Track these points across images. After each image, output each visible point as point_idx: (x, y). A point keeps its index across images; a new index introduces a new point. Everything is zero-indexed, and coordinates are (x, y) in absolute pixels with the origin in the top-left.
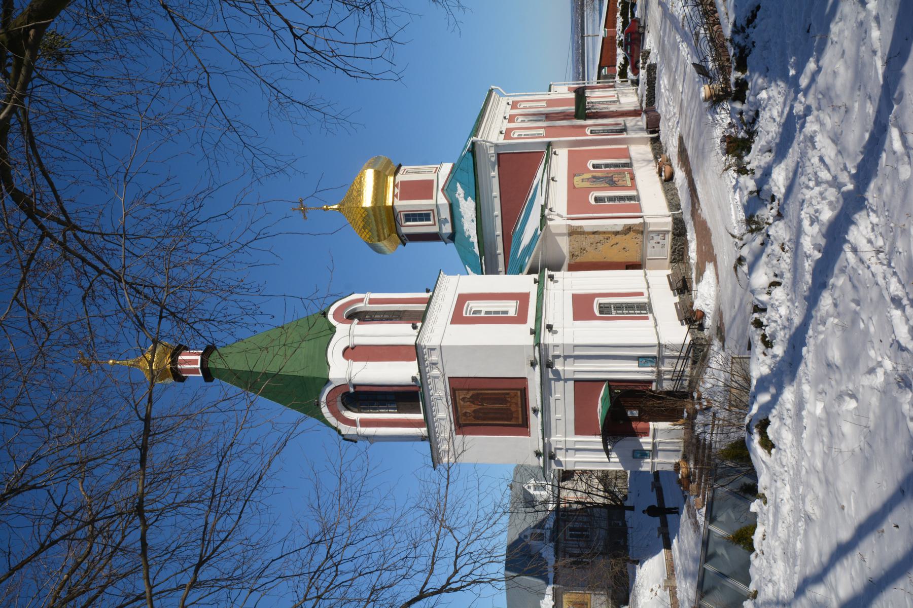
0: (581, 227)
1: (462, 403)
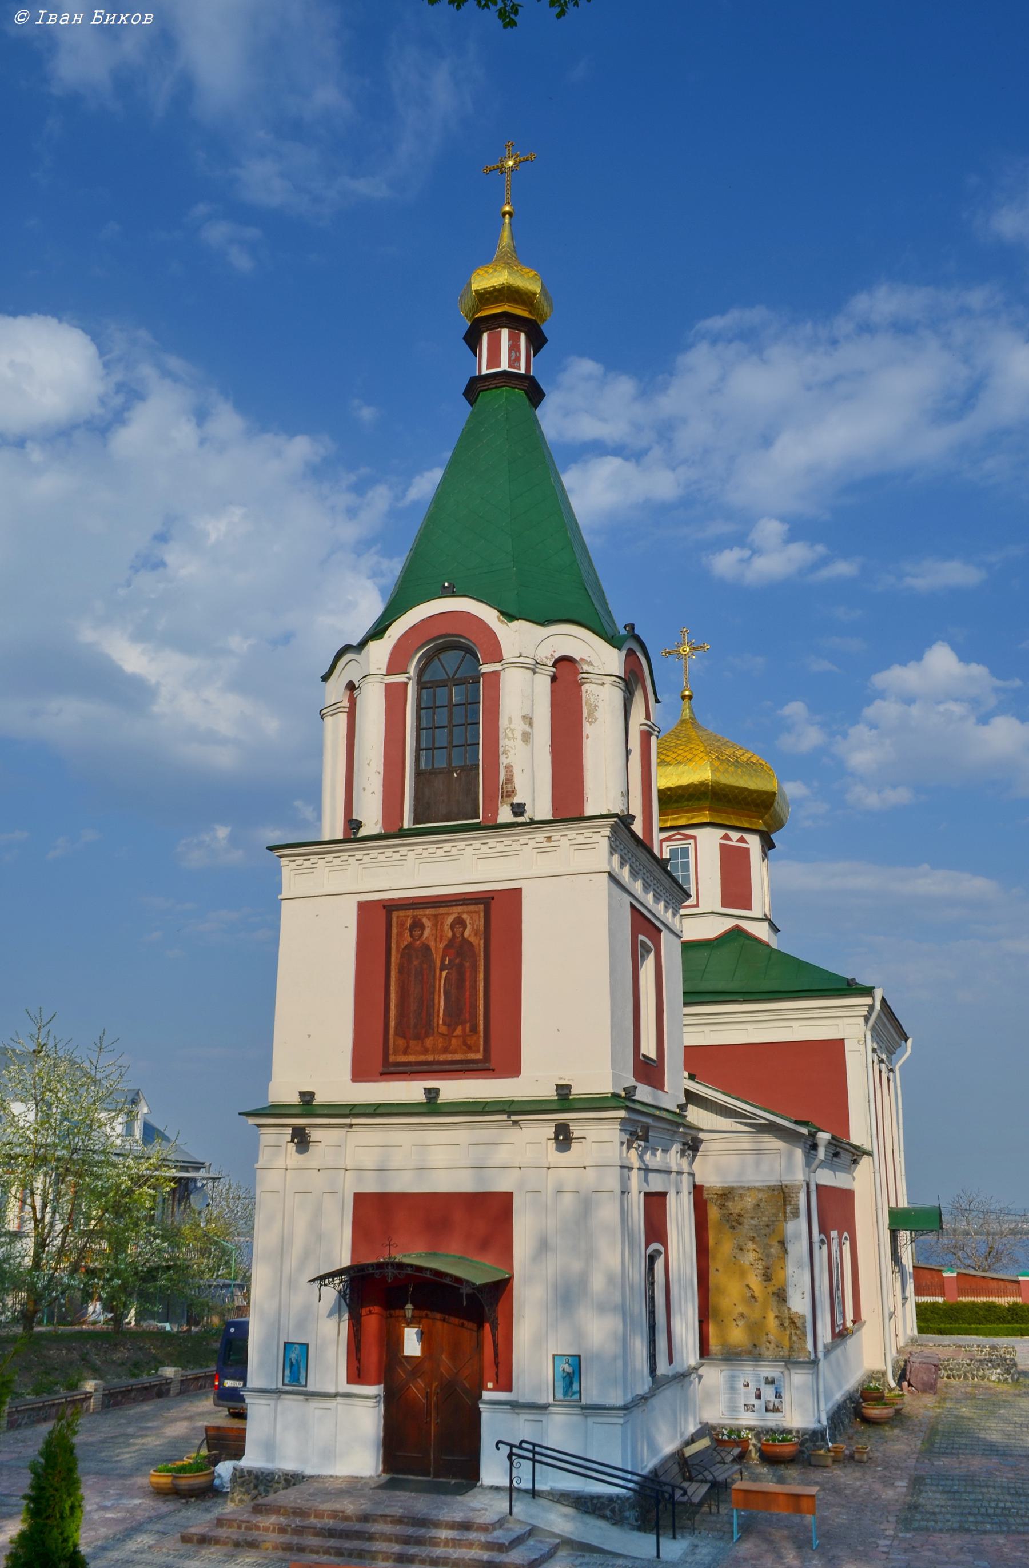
1: (450, 920)
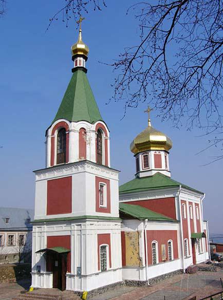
0: (141, 237)
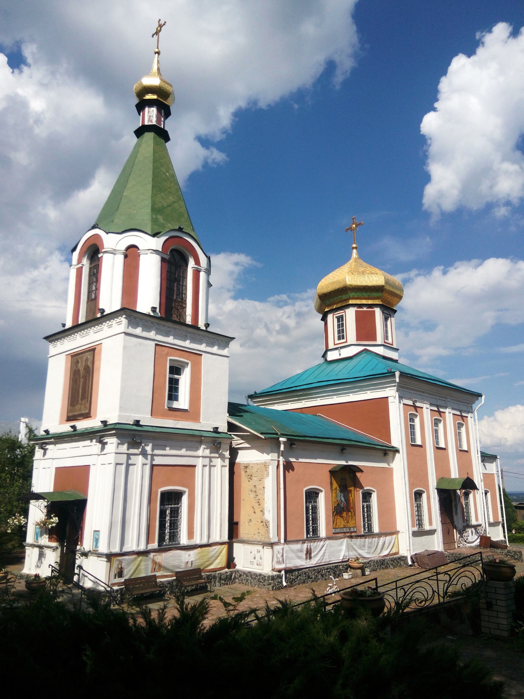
1: (85, 358)
